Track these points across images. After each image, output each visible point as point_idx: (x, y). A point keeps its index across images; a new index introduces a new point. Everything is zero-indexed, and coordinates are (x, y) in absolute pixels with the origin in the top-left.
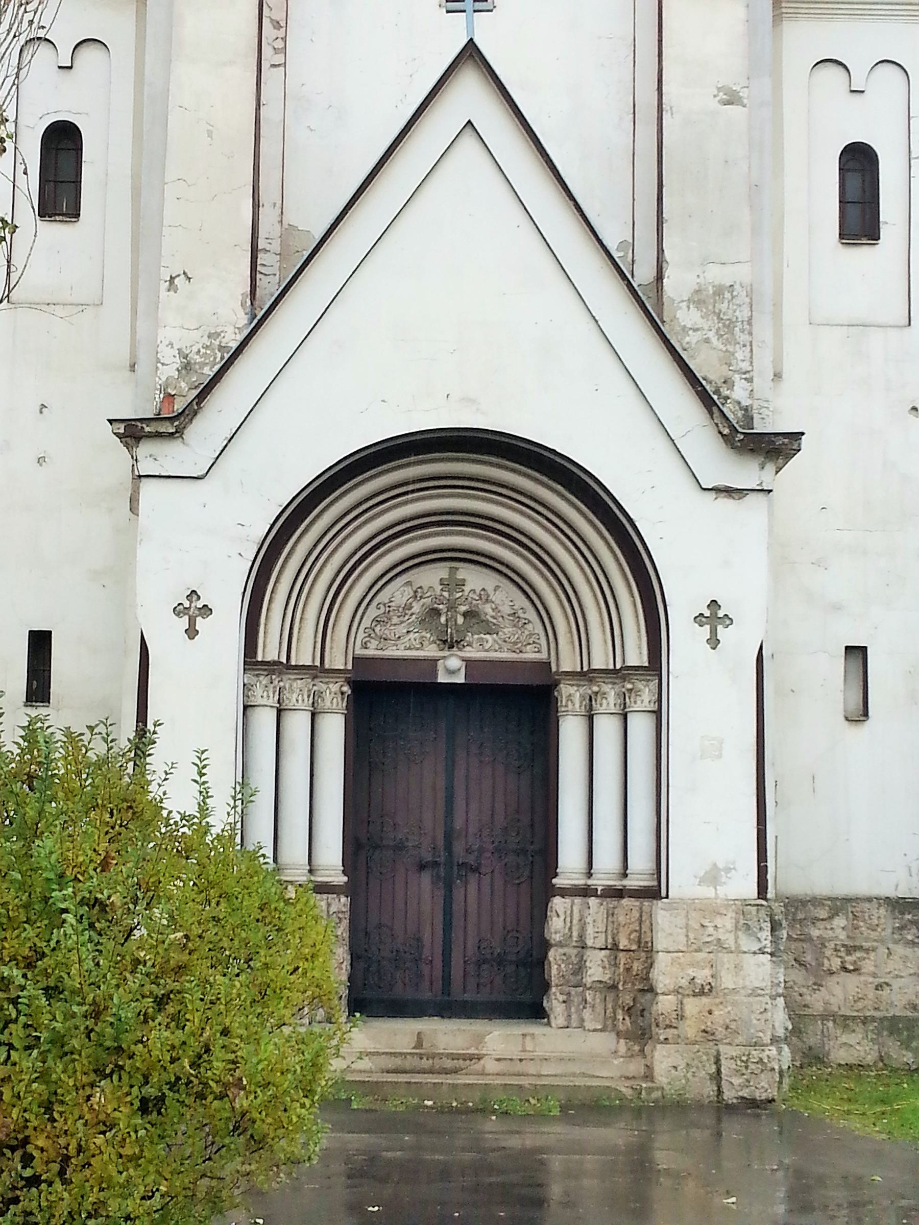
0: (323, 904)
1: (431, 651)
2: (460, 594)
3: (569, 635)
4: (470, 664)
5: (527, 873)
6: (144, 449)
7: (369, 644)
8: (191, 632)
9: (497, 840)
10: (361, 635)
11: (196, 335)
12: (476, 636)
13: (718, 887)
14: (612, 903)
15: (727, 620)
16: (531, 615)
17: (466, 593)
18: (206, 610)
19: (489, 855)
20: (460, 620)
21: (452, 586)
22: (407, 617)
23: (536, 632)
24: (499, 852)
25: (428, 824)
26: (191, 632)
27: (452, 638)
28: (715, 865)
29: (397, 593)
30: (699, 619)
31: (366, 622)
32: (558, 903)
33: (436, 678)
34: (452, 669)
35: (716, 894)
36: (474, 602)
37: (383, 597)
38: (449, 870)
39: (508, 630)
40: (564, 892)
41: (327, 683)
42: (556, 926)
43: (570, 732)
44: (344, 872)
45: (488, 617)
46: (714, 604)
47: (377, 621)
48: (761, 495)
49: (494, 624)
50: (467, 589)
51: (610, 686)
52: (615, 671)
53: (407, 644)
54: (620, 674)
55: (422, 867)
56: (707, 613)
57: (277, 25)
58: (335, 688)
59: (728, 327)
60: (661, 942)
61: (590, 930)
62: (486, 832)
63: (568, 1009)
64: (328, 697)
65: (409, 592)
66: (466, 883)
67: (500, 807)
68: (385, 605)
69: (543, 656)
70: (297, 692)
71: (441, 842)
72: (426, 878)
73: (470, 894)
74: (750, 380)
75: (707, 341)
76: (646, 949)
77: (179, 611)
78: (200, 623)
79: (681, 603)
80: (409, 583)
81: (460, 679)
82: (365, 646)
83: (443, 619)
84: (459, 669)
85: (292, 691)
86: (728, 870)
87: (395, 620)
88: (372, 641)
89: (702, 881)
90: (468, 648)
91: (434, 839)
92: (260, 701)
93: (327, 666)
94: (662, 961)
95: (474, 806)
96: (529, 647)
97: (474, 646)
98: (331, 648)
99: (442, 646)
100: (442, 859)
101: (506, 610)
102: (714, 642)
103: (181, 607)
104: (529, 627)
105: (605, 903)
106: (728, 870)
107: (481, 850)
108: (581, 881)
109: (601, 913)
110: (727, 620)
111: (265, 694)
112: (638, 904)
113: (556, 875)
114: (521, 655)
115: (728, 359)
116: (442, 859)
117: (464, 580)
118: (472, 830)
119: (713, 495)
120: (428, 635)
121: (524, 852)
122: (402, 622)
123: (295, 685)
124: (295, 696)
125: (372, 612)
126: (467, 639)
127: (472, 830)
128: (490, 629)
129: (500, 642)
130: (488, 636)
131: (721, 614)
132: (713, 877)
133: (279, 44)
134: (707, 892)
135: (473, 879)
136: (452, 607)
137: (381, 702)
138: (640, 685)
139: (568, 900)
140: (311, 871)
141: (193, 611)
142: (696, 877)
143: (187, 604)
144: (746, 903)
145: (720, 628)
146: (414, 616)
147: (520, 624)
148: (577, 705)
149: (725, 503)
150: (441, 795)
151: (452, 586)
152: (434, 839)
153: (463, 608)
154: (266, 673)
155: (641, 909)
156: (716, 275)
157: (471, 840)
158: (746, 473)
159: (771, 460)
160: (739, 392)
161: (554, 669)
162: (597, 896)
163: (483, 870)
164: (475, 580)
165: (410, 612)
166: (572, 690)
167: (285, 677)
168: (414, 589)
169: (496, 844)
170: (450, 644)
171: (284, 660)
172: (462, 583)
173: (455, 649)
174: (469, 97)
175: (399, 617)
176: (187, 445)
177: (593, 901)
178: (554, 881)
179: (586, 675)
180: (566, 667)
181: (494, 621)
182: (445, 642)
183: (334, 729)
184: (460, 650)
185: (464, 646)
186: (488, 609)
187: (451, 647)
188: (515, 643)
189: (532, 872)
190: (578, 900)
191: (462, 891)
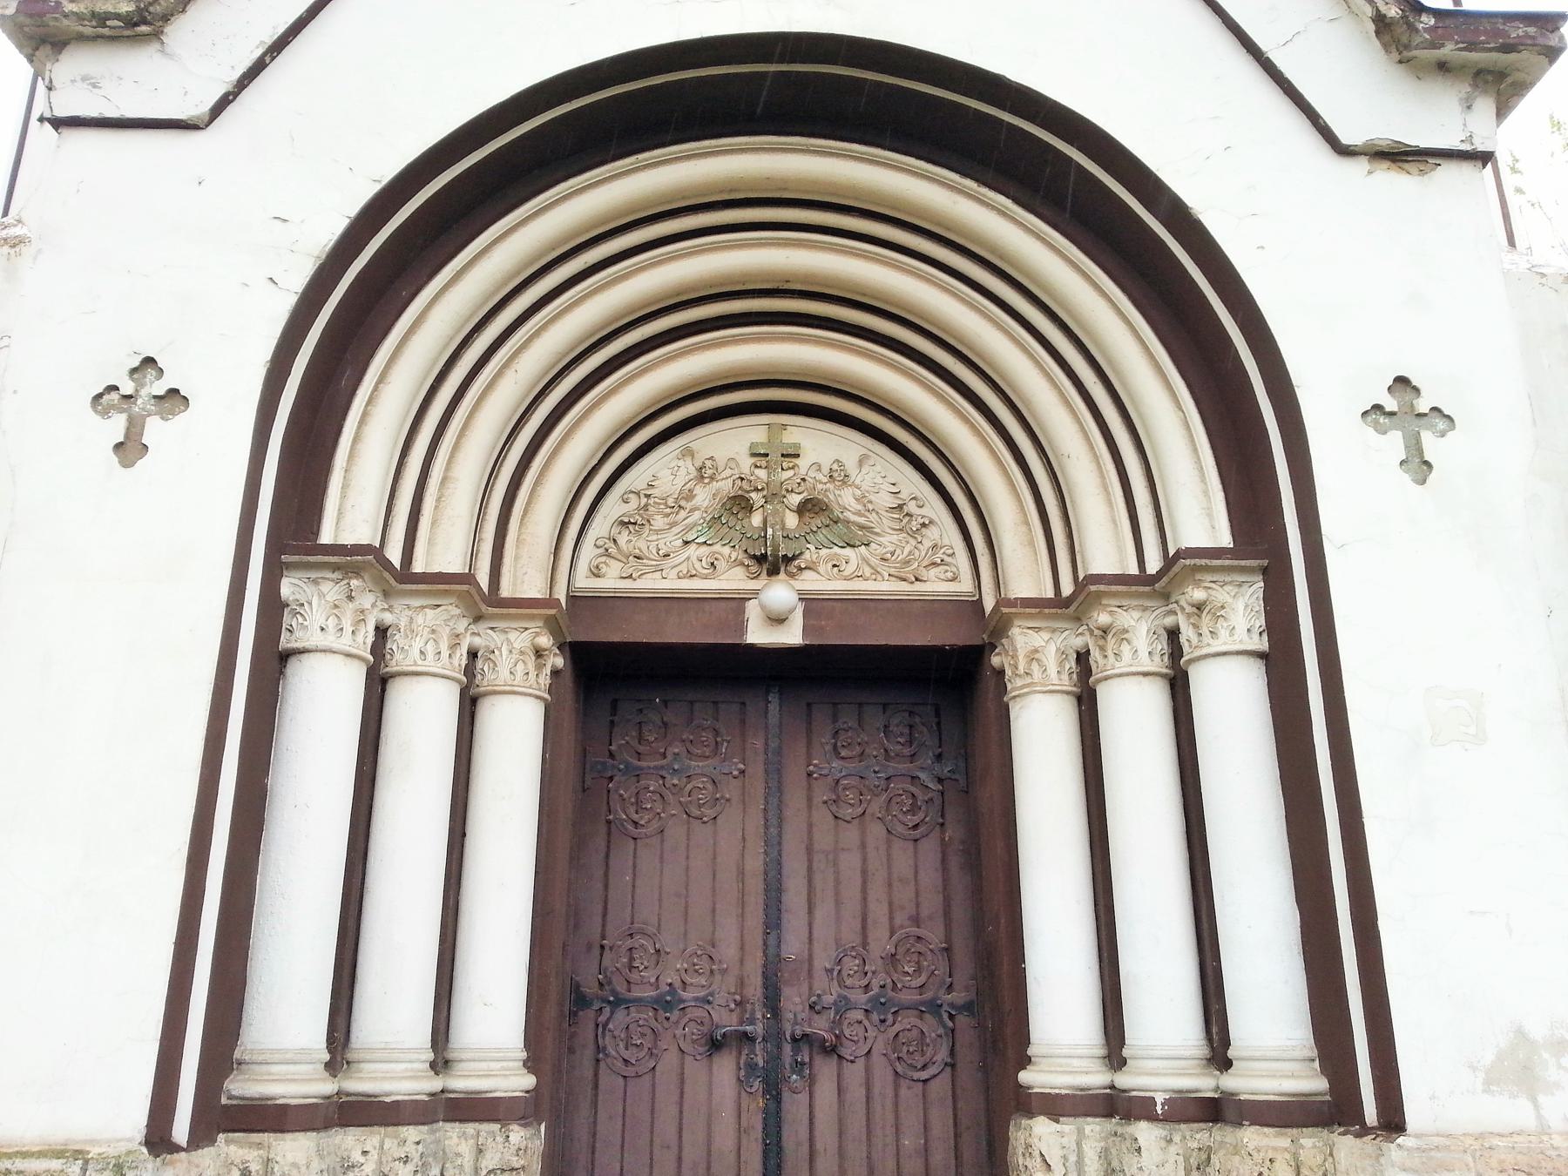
0: (466, 1149)
1: (733, 580)
2: (791, 473)
3: (1024, 529)
4: (813, 605)
5: (942, 1055)
6: (71, 66)
7: (604, 569)
8: (130, 449)
9: (875, 984)
10: (588, 551)
12: (824, 552)
13: (1541, 1099)
14: (1199, 1135)
16: (935, 508)
17: (803, 471)
18: (174, 398)
19: (859, 1015)
20: (792, 520)
21: (775, 456)
22: (683, 514)
23: (946, 542)
24: (882, 1007)
25: (728, 951)
26: (130, 449)
27: (776, 549)
28: (1520, 1033)
29: (664, 469)
31: (601, 526)
34: (775, 618)
35: (1539, 1117)
36: (820, 486)
37: (636, 477)
38: (777, 1055)
39: (888, 540)
40: (1057, 1106)
41: (504, 631)
43: (1040, 735)
44: (531, 1064)
45: (848, 514)
48: (1466, 170)
49: (862, 527)
50: (803, 463)
51: (1136, 614)
52: (1143, 579)
54: (1165, 579)
55: (715, 1045)
56: (1391, 404)
62: (851, 964)
64: (504, 660)
65: (687, 469)
66: (812, 1081)
67: (879, 911)
68: (638, 494)
69: (965, 586)
70: (428, 637)
71: (755, 989)
72: (725, 1068)
73: (822, 1103)
78: (155, 431)
80: (688, 453)
81: (792, 635)
82: (596, 573)
83: (756, 519)
84: (792, 611)
85: (412, 632)
87: (659, 522)
88: (612, 562)
89: (1492, 1081)
90: (807, 574)
91: (741, 983)
92: (311, 638)
93: (506, 591)
95: (824, 911)
96: (933, 572)
97: (821, 569)
98: (517, 558)
99: (754, 569)
100: (758, 1029)
102: (1419, 466)
103: (114, 396)
104: (932, 534)
105: (1177, 1138)
107: (843, 1006)
108: (1096, 1078)
109: (1170, 1167)
111: (332, 622)
112: (1284, 1142)
113: (1025, 1061)
114: (918, 587)
116: (758, 1029)
117: (797, 446)
118: (823, 961)
119: (1362, 164)
120: (726, 550)
121: (934, 1007)
122: (672, 525)
123: (420, 619)
124: (418, 644)
125: (613, 507)
126: (807, 555)
127: (823, 961)
129: (874, 561)
130: (848, 551)
134: (1509, 1112)
135: (826, 1070)
136: (774, 495)
138: (1222, 595)
139: (1068, 1126)
140: (441, 1063)
141: (139, 401)
142: (1474, 1069)
143: (127, 387)
145: (1427, 438)
146: (697, 515)
147: (915, 525)
148: (1053, 669)
150: (756, 886)
151: (775, 456)
152: (741, 983)
153: (795, 500)
154: (337, 575)
155: (1296, 1156)
157: (821, 982)
158: (1435, 117)
159: (1485, 92)
161: (989, 604)
162: (1152, 1117)
163: (846, 1052)
164: (820, 447)
165: (689, 506)
166: (1038, 639)
167: (399, 603)
168: (698, 464)
169: (875, 990)
170: (772, 563)
171: (394, 555)
173: (782, 575)
175: (667, 515)
176: (170, 56)
177: (1146, 1133)
178: (1025, 1077)
181: (861, 520)
182: (760, 559)
183: (516, 735)
184: (792, 575)
185: (800, 569)
186: (846, 500)
187: (773, 572)
188: (907, 563)
189: (952, 1053)
190: (1094, 1127)
191: (803, 1098)
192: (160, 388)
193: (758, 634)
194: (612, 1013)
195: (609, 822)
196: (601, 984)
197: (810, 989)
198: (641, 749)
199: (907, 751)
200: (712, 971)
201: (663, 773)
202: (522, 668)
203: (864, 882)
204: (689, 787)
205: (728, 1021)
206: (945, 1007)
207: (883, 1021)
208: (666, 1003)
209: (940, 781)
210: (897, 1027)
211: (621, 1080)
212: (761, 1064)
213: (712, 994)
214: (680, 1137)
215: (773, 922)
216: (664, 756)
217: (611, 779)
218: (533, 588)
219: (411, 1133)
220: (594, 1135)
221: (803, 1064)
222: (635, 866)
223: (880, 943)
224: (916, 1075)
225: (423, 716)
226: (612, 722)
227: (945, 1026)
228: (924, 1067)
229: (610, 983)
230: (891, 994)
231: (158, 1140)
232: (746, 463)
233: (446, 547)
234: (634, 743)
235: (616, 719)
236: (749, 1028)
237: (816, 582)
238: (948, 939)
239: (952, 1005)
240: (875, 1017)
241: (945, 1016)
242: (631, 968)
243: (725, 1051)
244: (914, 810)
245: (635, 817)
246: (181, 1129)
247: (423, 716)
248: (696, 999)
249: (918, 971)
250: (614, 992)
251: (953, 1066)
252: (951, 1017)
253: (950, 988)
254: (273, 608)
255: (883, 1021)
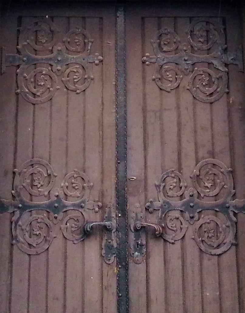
5: (230, 238)
9: (187, 194)
19: (177, 214)
24: (191, 209)
25: (94, 175)
38: (125, 239)
55: (86, 234)
62: (171, 182)
66: (147, 256)
67: (188, 148)
71: (111, 199)
72: (93, 249)
73: (154, 270)
91: (102, 194)
95: (154, 149)
100: (113, 224)
107: (167, 208)
116: (113, 224)
118: (153, 180)
121: (224, 208)
127: (153, 180)
135: (156, 249)
150: (110, 133)
152: (102, 194)
157: (152, 193)
163: (169, 237)
169: (187, 198)
189: (236, 237)
191: (143, 266)
194: (21, 214)
195: (17, 94)
196: (14, 197)
197: (146, 198)
198: (37, 47)
199: (205, 47)
200: (83, 188)
201: (51, 63)
203: (179, 130)
204: (68, 71)
205: (94, 219)
206: (231, 208)
207: (192, 218)
208: (55, 208)
209: (226, 65)
210: (201, 221)
211: (27, 257)
212: (115, 245)
213: (84, 202)
214: (65, 292)
215: (122, 156)
216: (52, 51)
217: (18, 67)
220: (10, 292)
221: (142, 245)
222: (34, 121)
223: (190, 168)
224: (214, 252)
226: (19, 31)
227: (231, 220)
228: (218, 246)
229: (19, 195)
230: (197, 200)
234: (33, 44)
235: (21, 29)
236: (107, 223)
238: (232, 165)
239: (235, 207)
240: (187, 215)
241: (231, 214)
242: (32, 186)
243: (92, 238)
244: (210, 83)
245: (34, 91)
248: (74, 205)
249: (214, 185)
250: (22, 201)
251: (237, 245)
252: (235, 214)
253: (234, 196)
255: (192, 218)
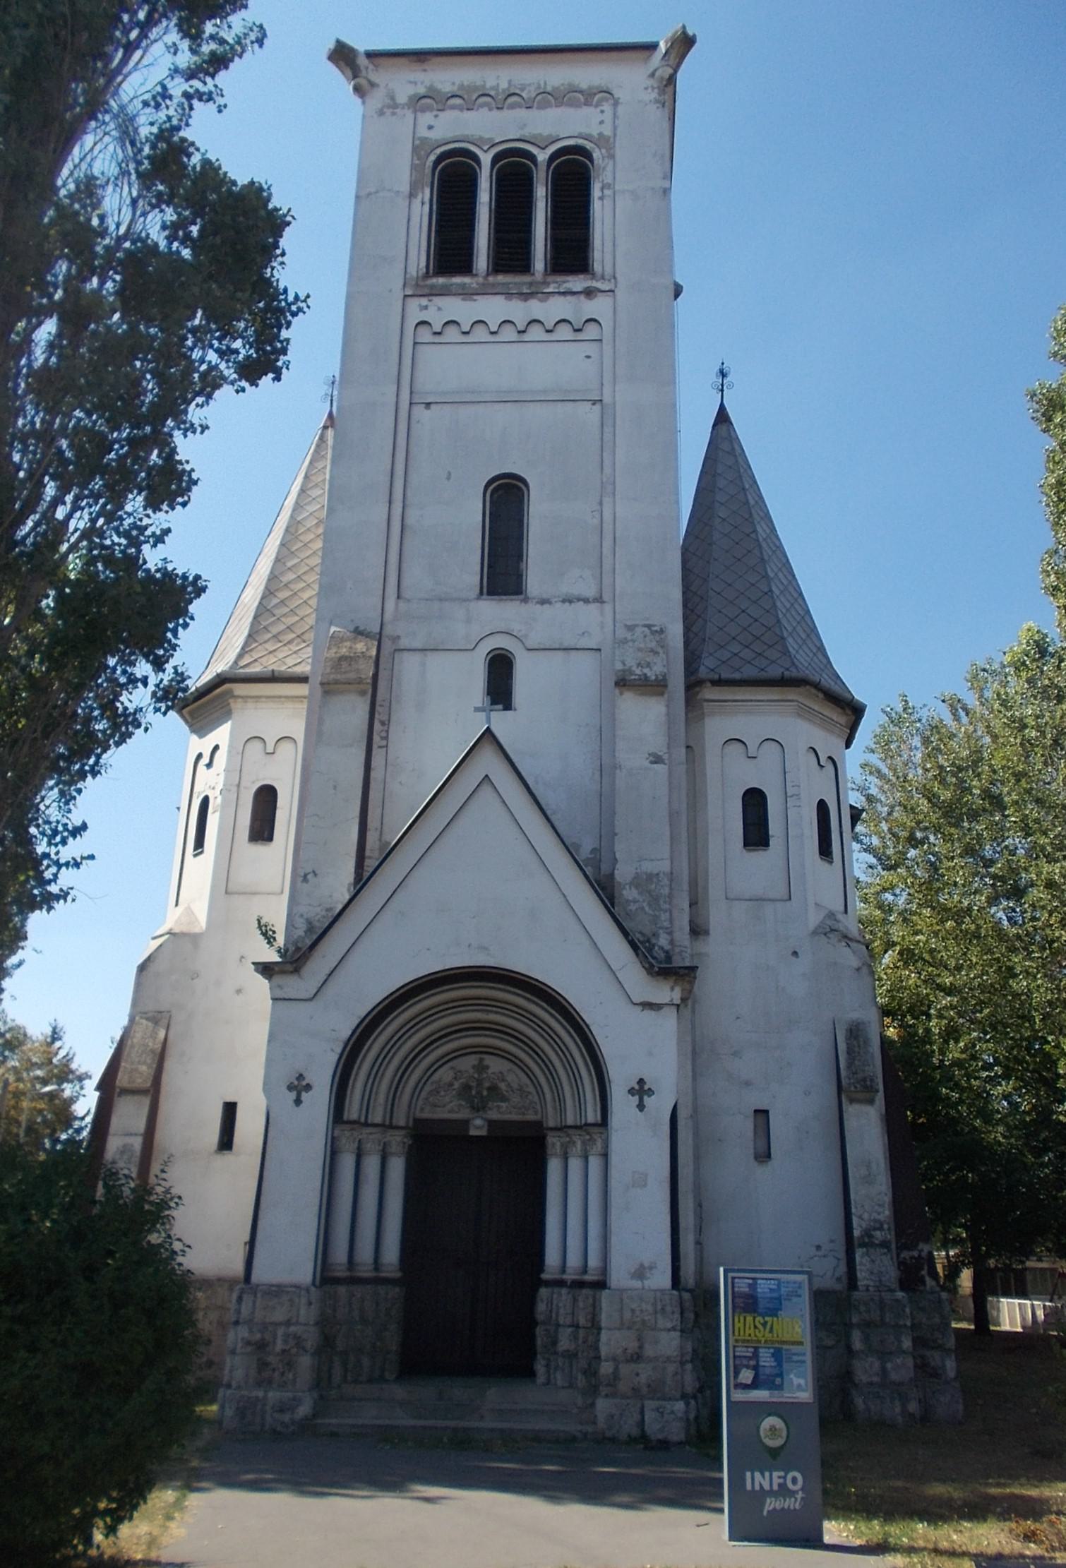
4: (492, 1124)
8: (298, 1102)
10: (420, 1102)
11: (318, 909)
15: (650, 1092)
16: (531, 1089)
18: (308, 1087)
20: (485, 1093)
26: (298, 1102)
28: (642, 1265)
29: (445, 1074)
30: (631, 1092)
31: (424, 1094)
32: (543, 1292)
33: (467, 1129)
34: (478, 1128)
37: (436, 1077)
39: (515, 1099)
40: (548, 1283)
42: (541, 1307)
44: (401, 1269)
46: (641, 1082)
47: (430, 1093)
50: (490, 1071)
53: (450, 1109)
54: (583, 1127)
57: (383, 723)
58: (399, 1139)
59: (655, 900)
60: (604, 1320)
61: (562, 1311)
63: (548, 1372)
65: (451, 1073)
69: (538, 1117)
74: (670, 933)
75: (643, 909)
76: (595, 1326)
77: (290, 1088)
79: (620, 1078)
81: (483, 1133)
82: (422, 1109)
83: (474, 1092)
86: (651, 1268)
94: (604, 1336)
101: (515, 1086)
102: (641, 1107)
106: (651, 1268)
108: (557, 1276)
110: (650, 1092)
115: (655, 919)
125: (428, 1088)
128: (504, 1099)
131: (646, 1087)
132: (640, 1273)
133: (384, 734)
134: (637, 1284)
136: (480, 1083)
137: (432, 1149)
139: (549, 1290)
144: (662, 1291)
145: (645, 1097)
149: (649, 1014)
153: (487, 1084)
156: (648, 867)
160: (663, 941)
164: (495, 1065)
166: (554, 1140)
170: (478, 1108)
172: (488, 1067)
174: (488, 762)
177: (564, 1291)
179: (562, 1129)
180: (551, 1124)
183: (397, 1168)
186: (503, 1086)
187: (478, 1110)
190: (556, 1290)
192: (304, 1083)
193: (473, 1132)
202: (397, 1140)
218: (402, 1123)
219: (369, 1287)
225: (372, 1165)
231: (313, 1283)
232: (471, 1071)
233: (377, 1117)
237: (493, 1115)
246: (318, 1282)
247: (372, 1165)
254: (333, 1138)
